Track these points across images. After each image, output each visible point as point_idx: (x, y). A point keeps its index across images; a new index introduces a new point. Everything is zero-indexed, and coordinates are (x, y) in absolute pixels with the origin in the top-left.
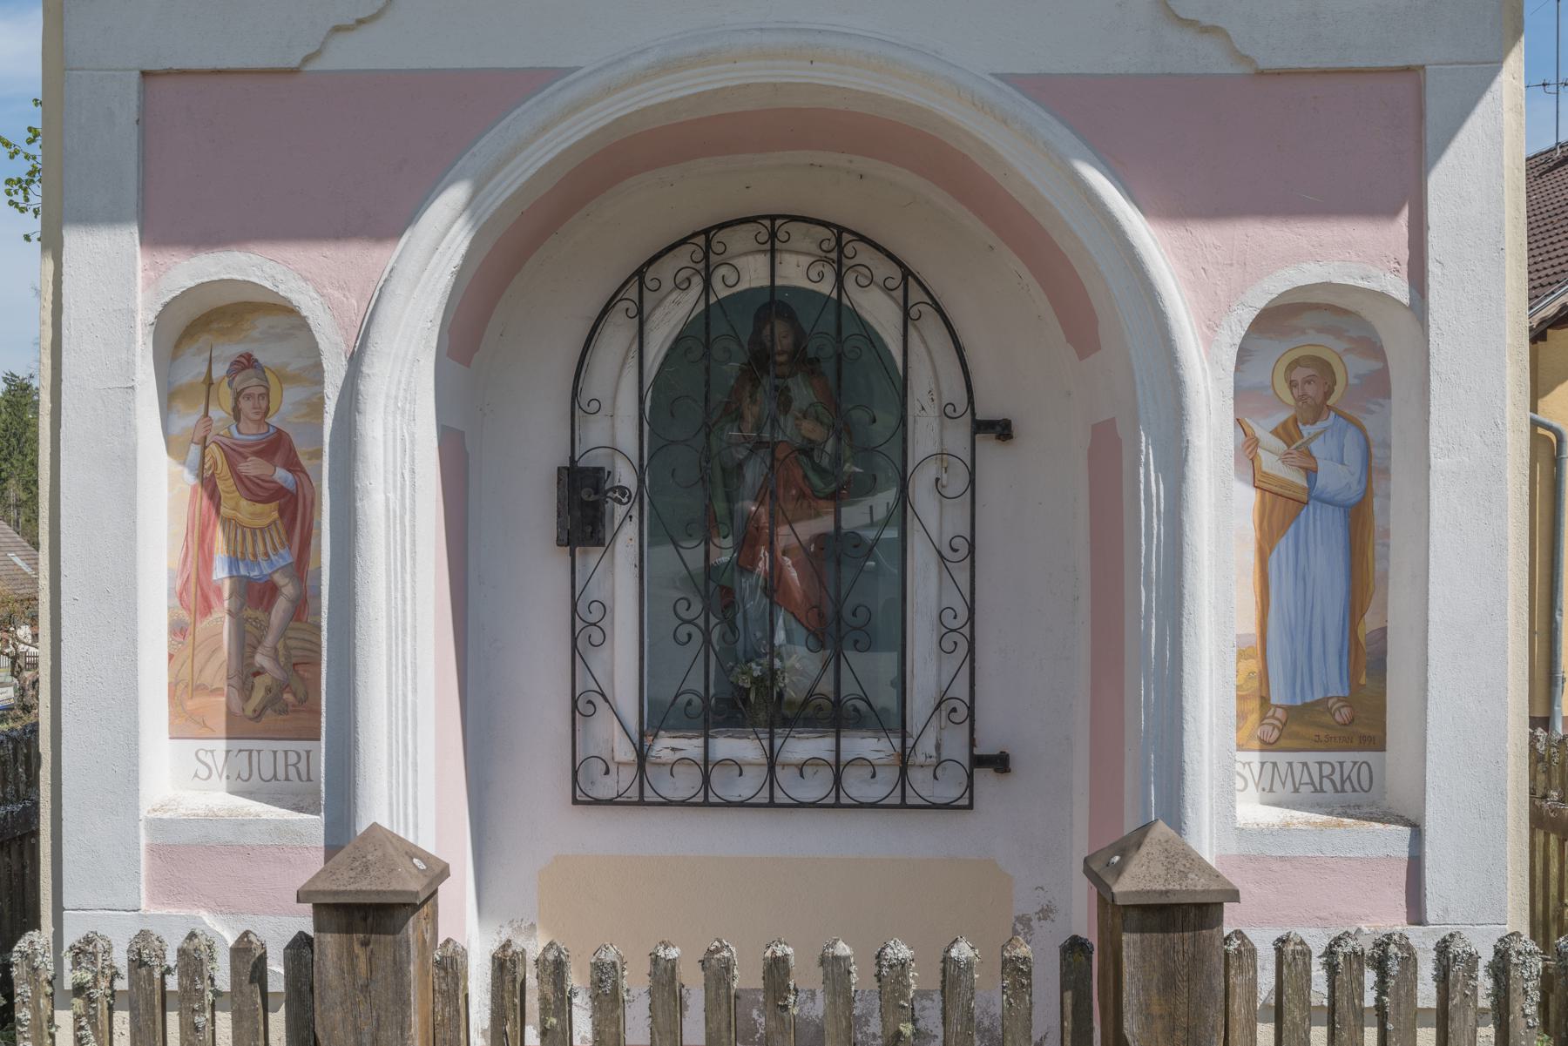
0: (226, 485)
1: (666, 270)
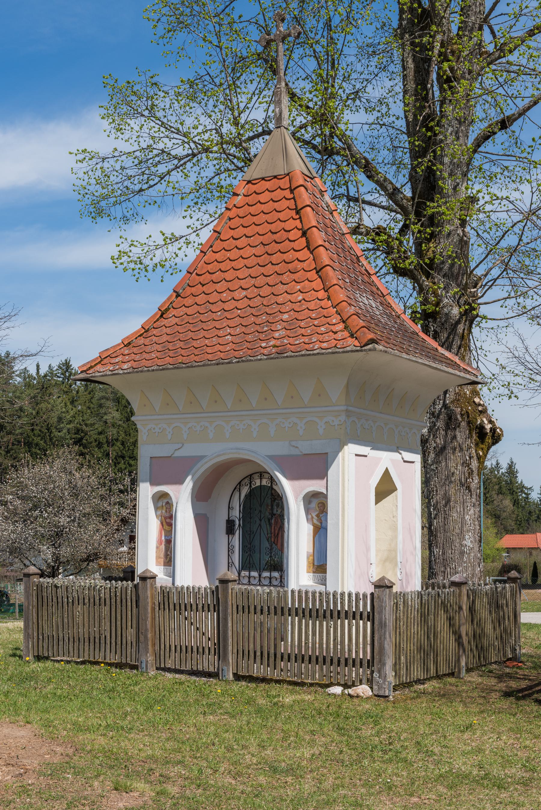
0: (164, 523)
1: (243, 483)
